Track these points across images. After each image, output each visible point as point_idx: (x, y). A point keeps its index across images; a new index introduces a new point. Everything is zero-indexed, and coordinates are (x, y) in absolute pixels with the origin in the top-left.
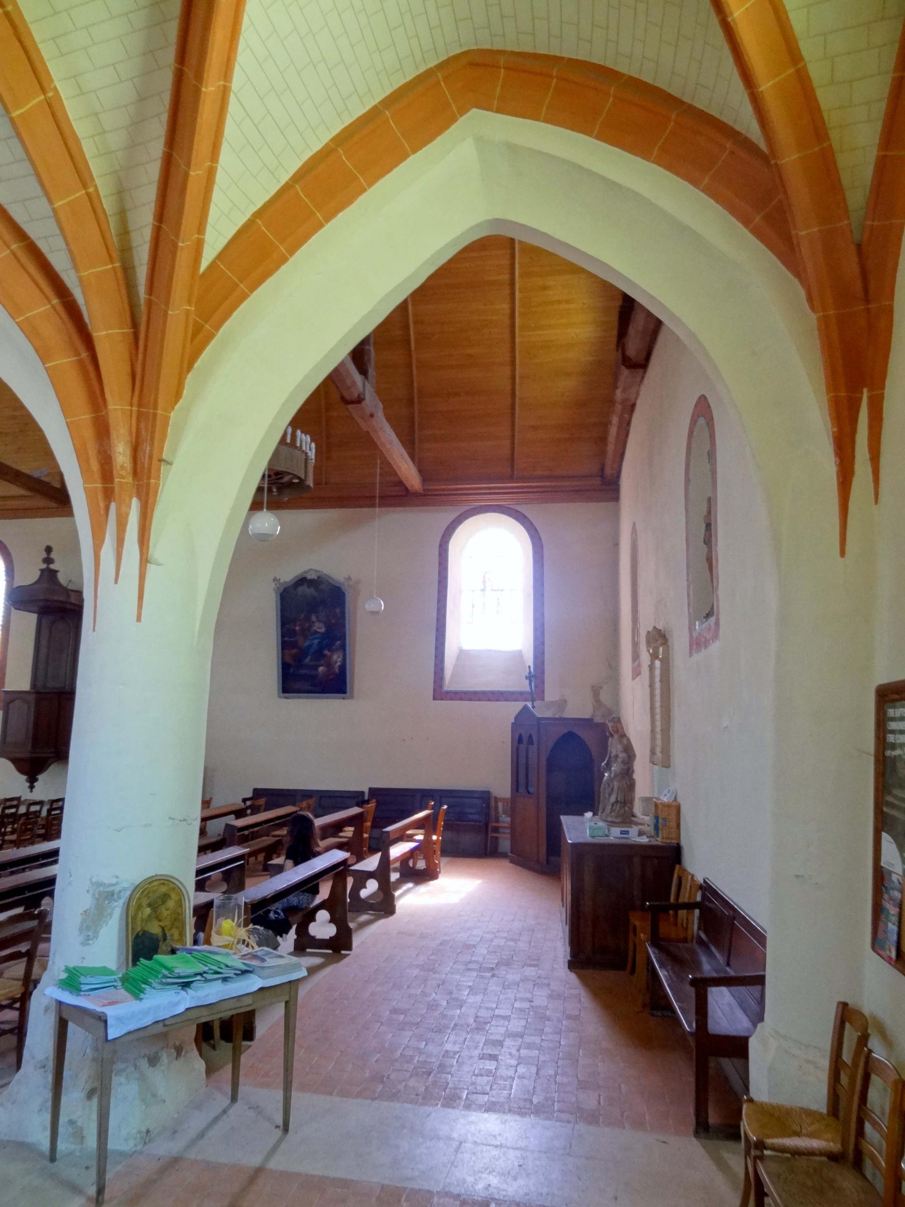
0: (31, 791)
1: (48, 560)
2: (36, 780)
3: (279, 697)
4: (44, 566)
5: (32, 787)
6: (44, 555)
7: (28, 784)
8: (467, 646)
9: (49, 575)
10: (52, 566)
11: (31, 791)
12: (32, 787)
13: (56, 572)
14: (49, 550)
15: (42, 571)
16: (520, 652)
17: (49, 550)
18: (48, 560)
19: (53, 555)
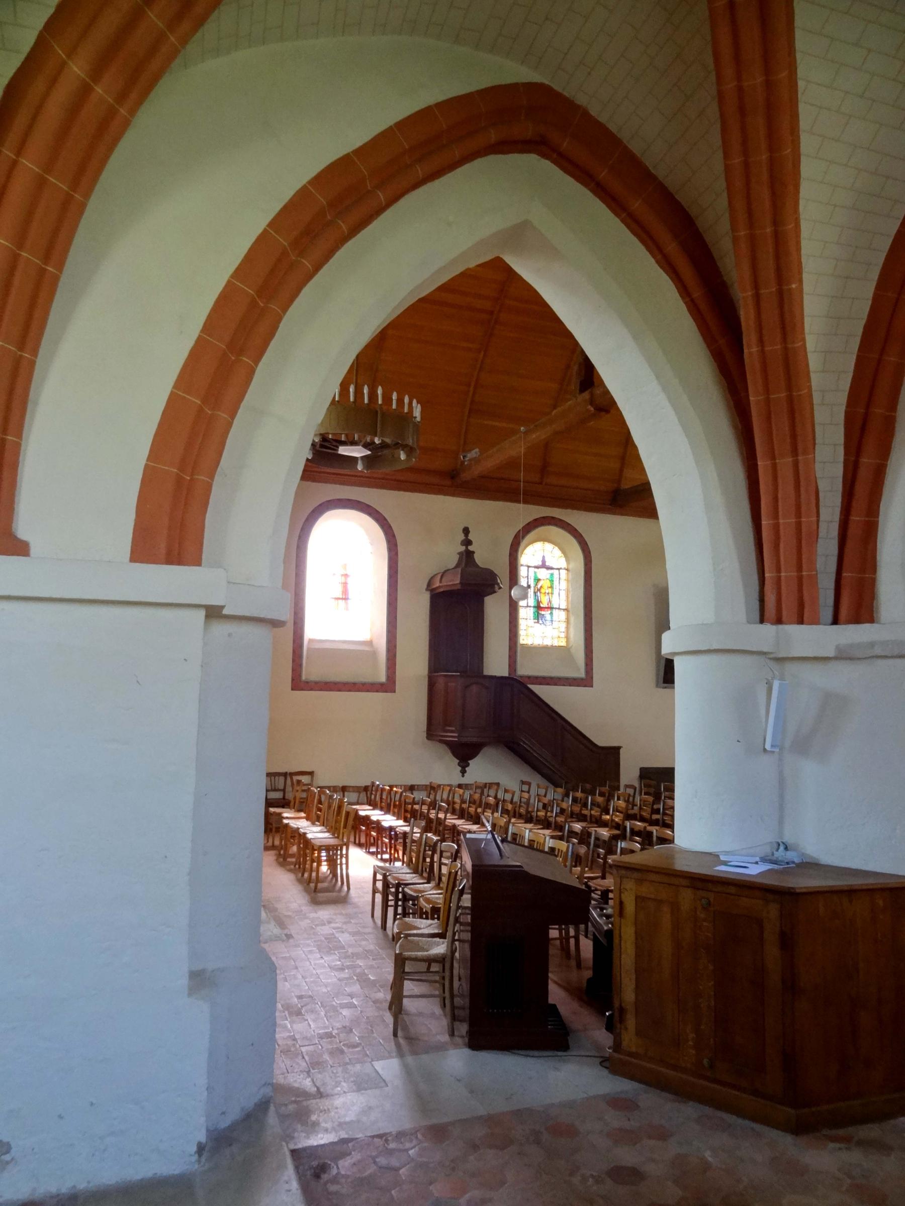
0: (463, 776)
1: (467, 542)
2: (468, 765)
3: (657, 686)
4: (463, 548)
5: (463, 772)
6: (462, 537)
7: (460, 768)
8: (312, 637)
9: (467, 557)
10: (470, 548)
11: (463, 776)
12: (463, 772)
13: (473, 552)
14: (466, 531)
15: (460, 554)
16: (370, 643)
17: (466, 531)
18: (467, 542)
19: (470, 537)
